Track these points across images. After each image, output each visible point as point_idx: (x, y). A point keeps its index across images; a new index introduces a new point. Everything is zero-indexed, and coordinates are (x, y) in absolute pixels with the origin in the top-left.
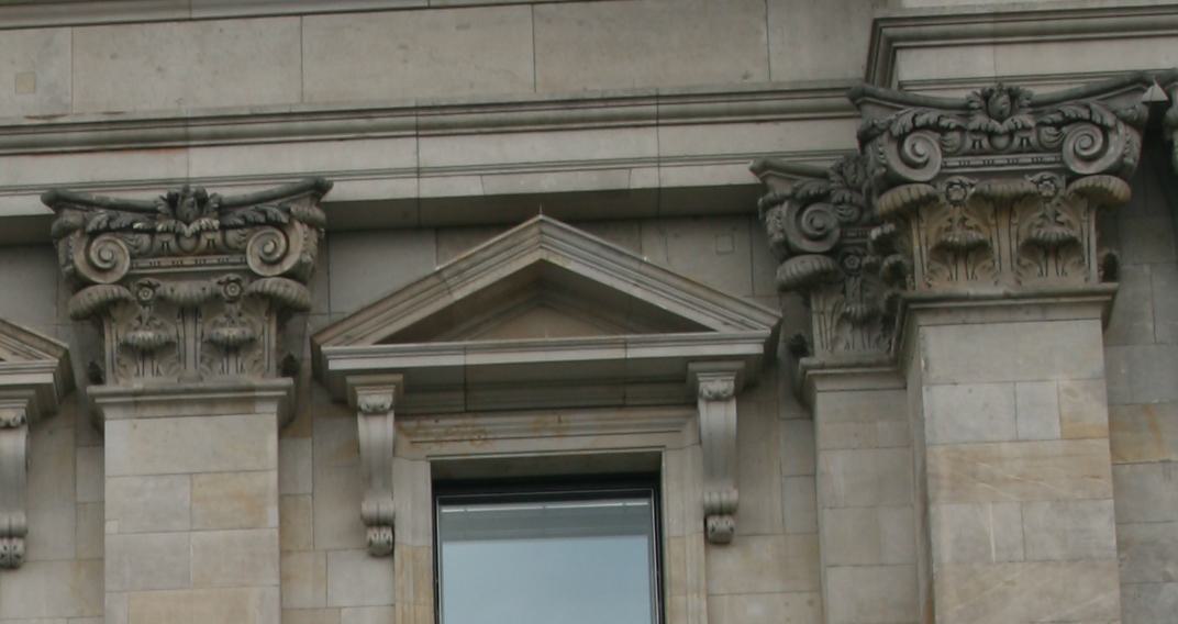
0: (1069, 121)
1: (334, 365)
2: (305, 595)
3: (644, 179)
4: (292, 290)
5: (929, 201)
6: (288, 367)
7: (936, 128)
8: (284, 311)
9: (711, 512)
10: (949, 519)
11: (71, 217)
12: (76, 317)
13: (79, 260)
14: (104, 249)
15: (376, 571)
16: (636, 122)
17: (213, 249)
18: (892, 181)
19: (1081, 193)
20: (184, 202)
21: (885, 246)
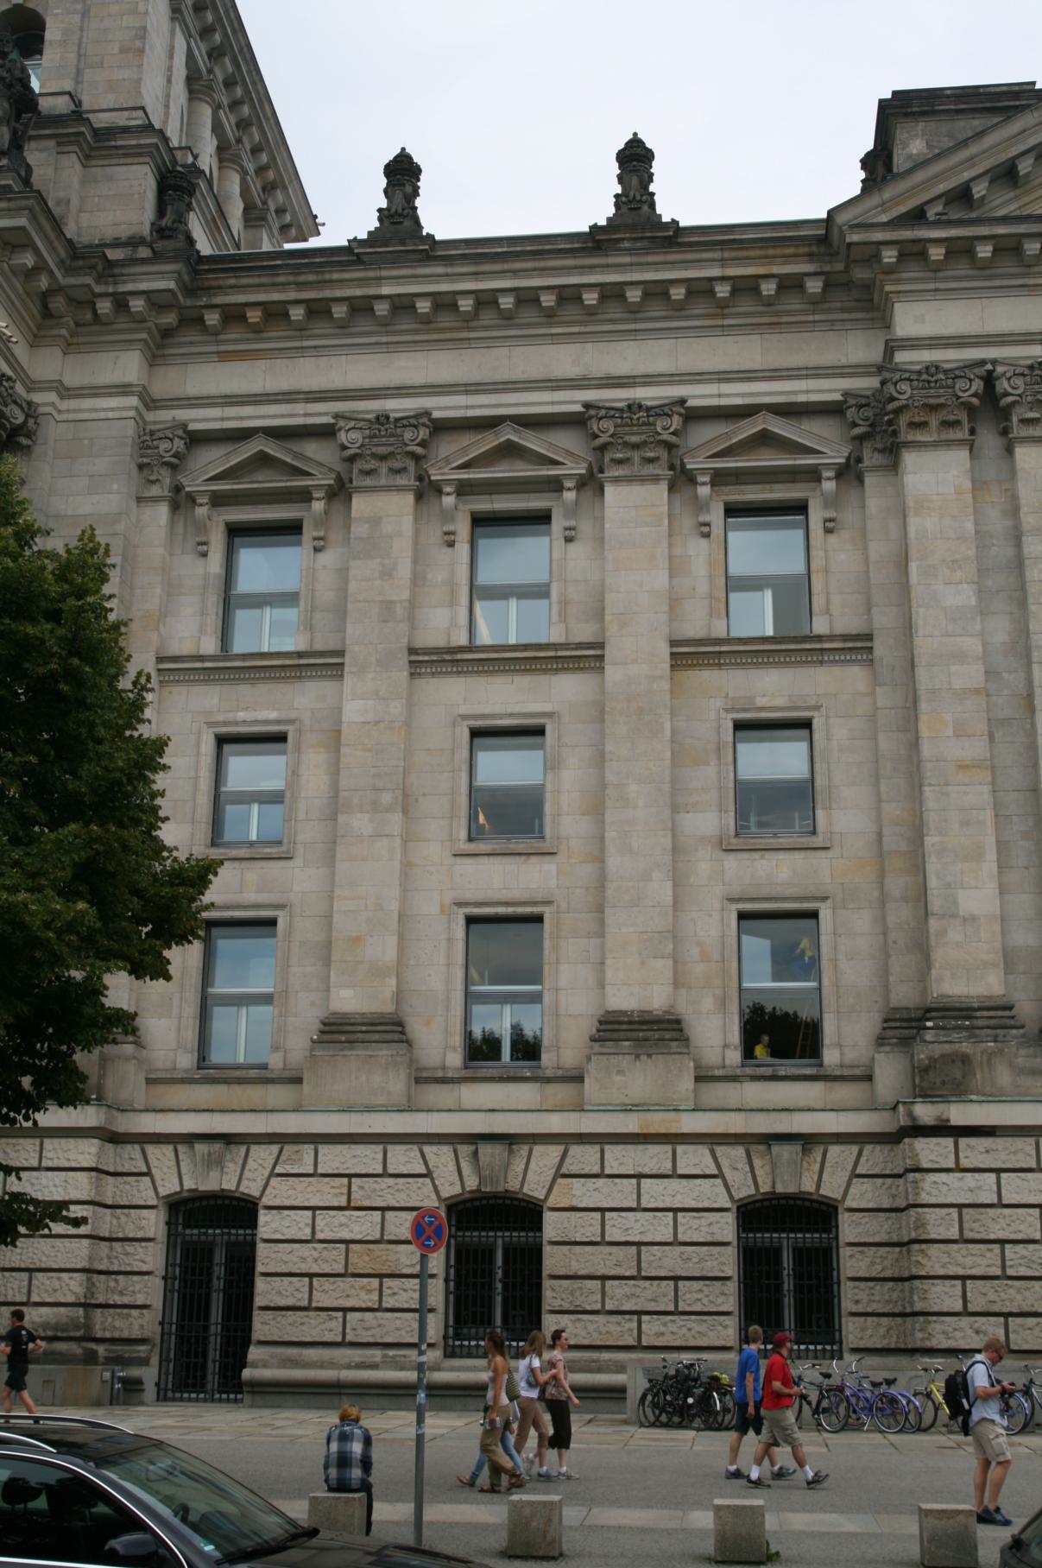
0: (957, 377)
1: (688, 467)
2: (678, 551)
3: (802, 398)
4: (673, 439)
5: (906, 406)
6: (672, 467)
7: (909, 379)
8: (670, 446)
9: (826, 521)
10: (914, 523)
11: (592, 412)
12: (594, 449)
13: (595, 428)
14: (605, 424)
15: (704, 542)
16: (799, 377)
17: (644, 424)
18: (893, 399)
19: (962, 403)
20: (634, 407)
21: (890, 423)
